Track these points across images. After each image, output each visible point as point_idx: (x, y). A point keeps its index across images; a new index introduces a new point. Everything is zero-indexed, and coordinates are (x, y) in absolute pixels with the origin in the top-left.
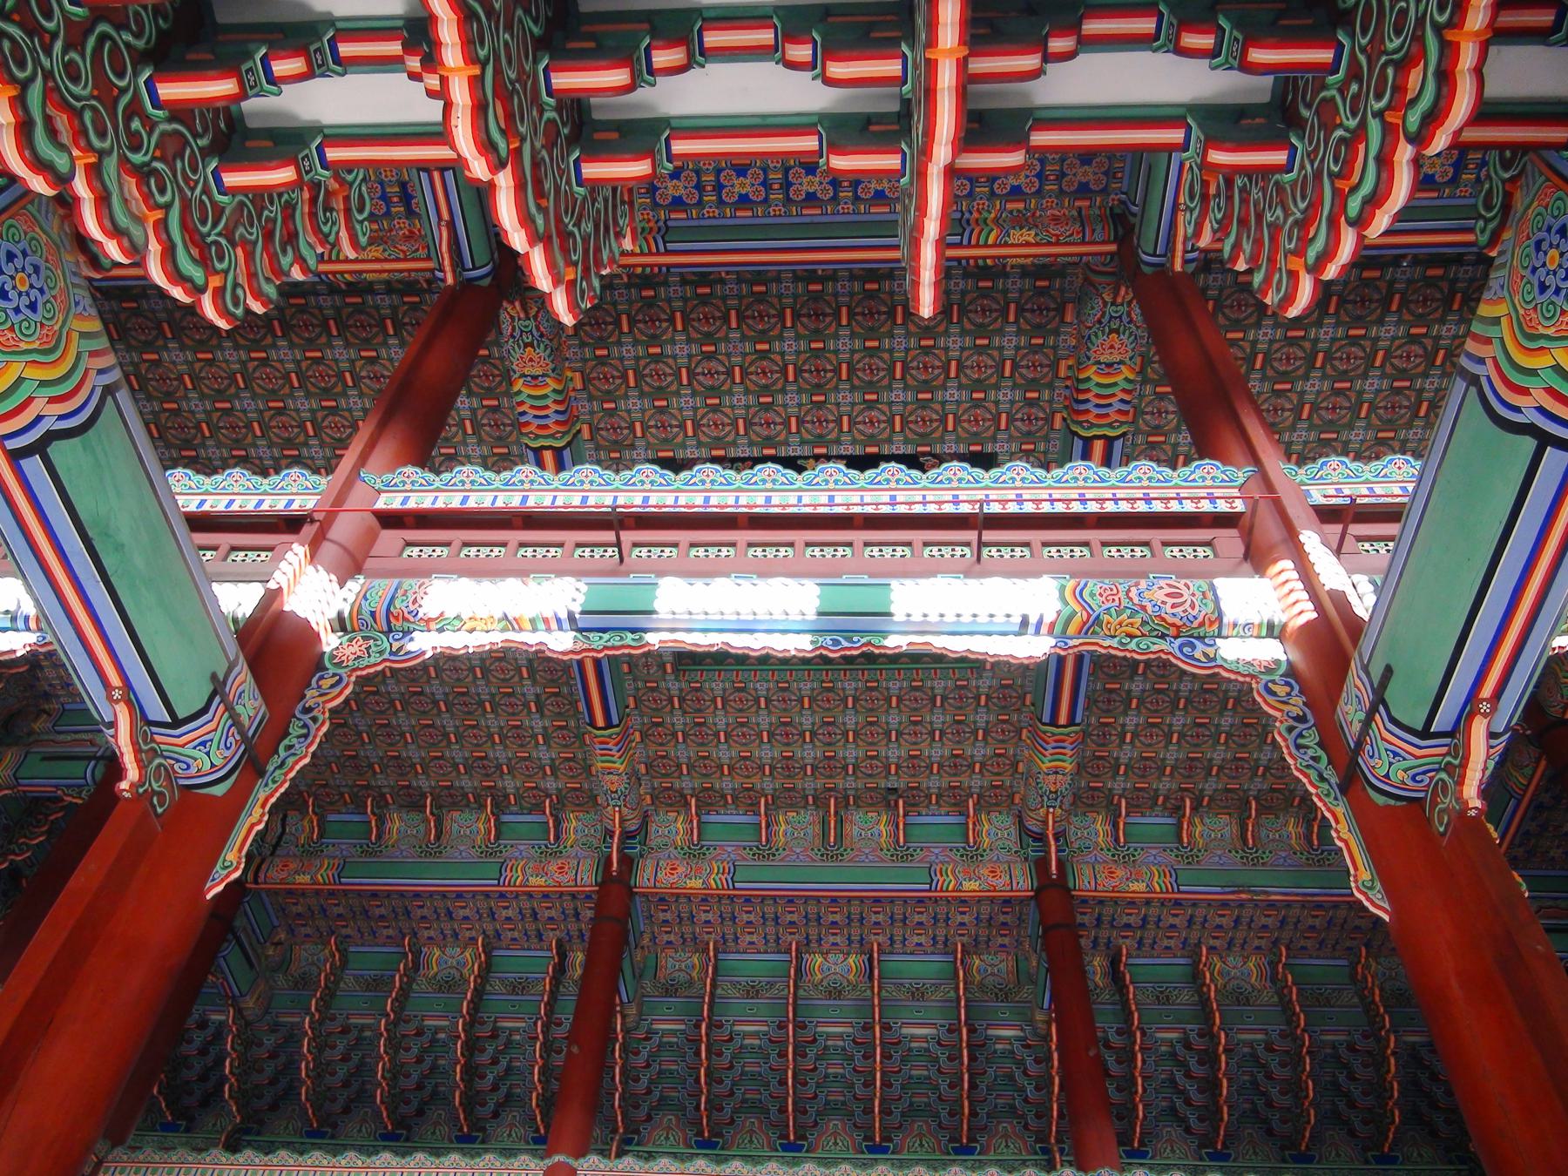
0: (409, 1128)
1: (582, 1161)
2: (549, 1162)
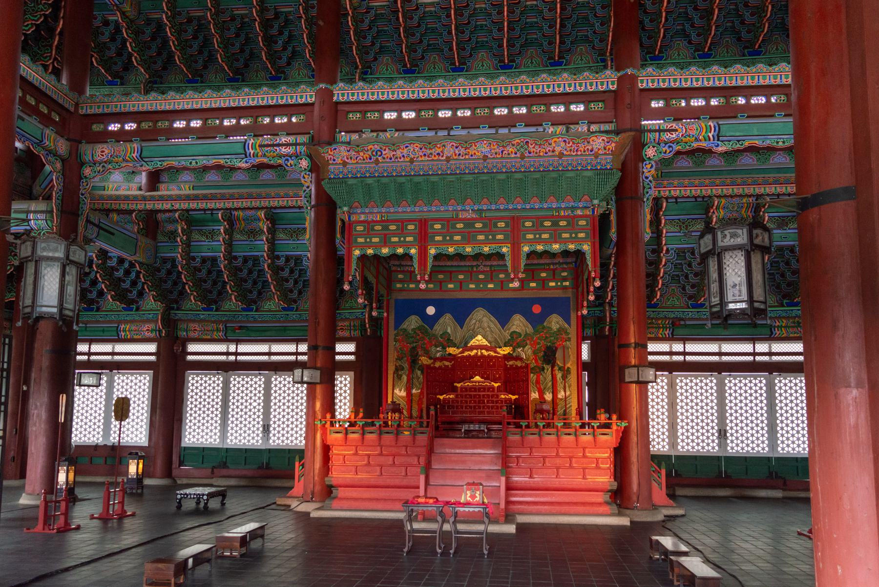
0: (242, 75)
1: (335, 86)
2: (317, 88)
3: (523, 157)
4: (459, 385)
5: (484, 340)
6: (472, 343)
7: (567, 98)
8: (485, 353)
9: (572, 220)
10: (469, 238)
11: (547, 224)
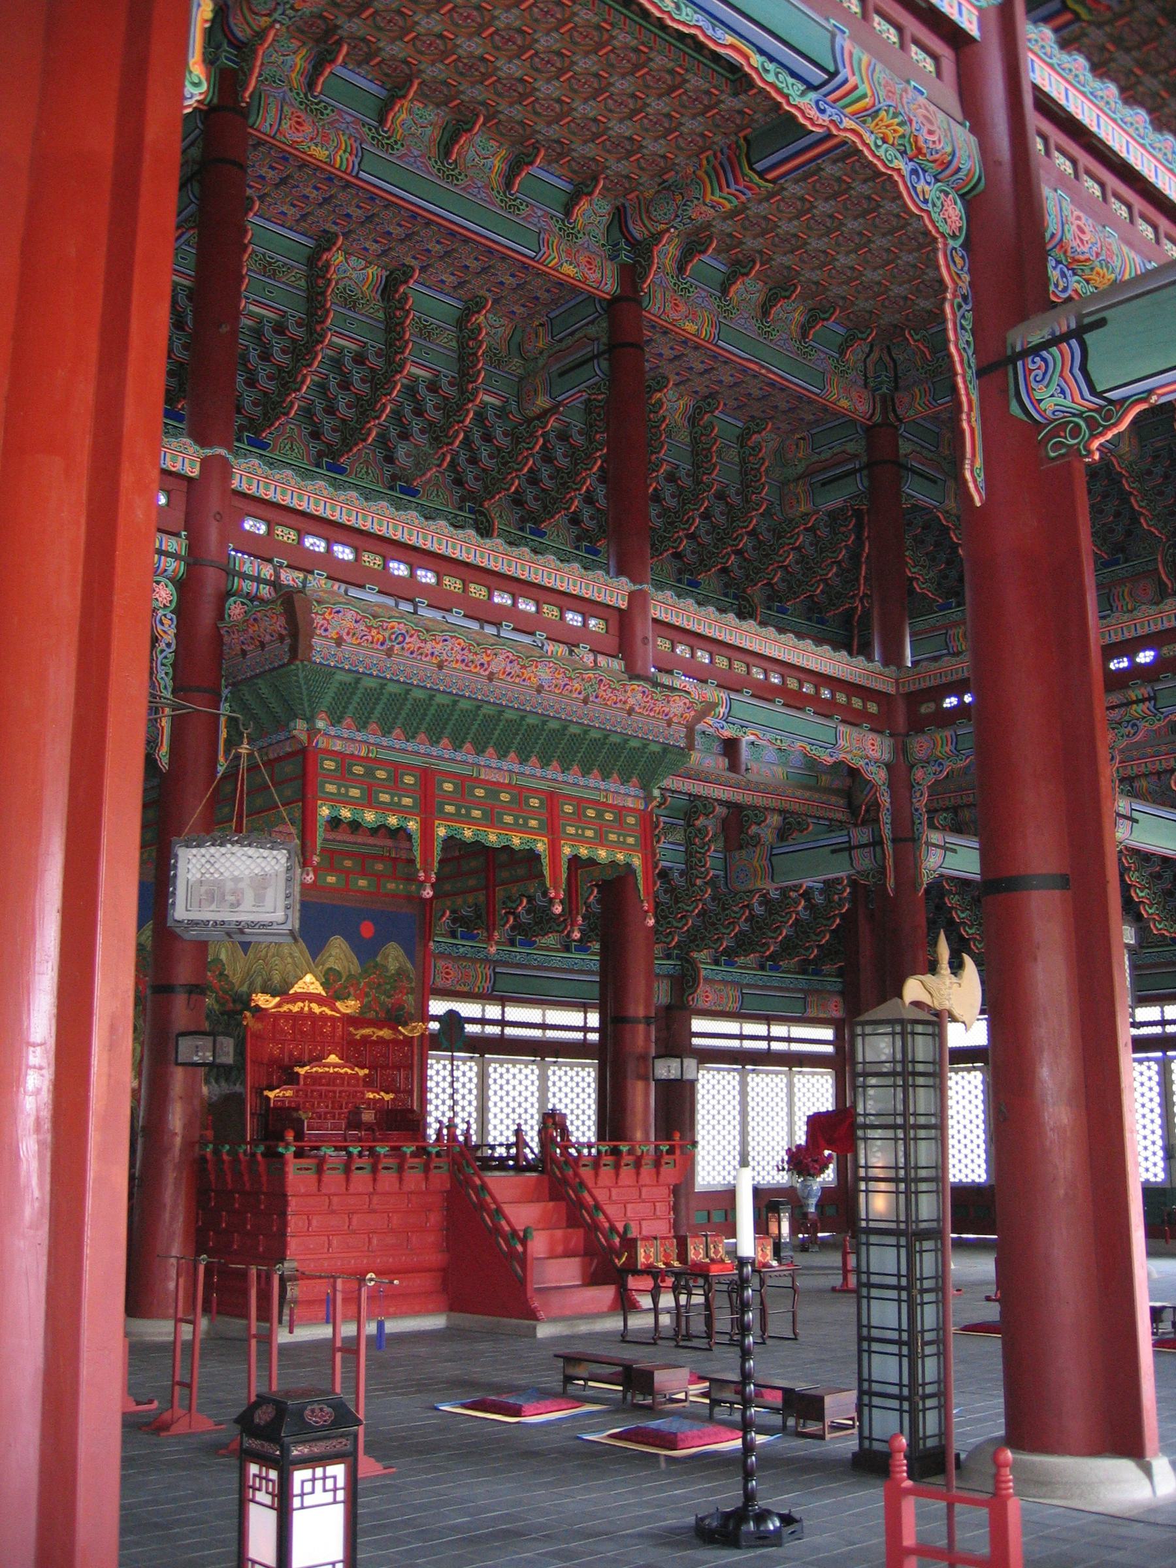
2: (209, 452)
3: (585, 701)
4: (302, 1071)
5: (317, 984)
6: (297, 988)
7: (333, 530)
8: (316, 1009)
9: (620, 811)
10: (492, 819)
11: (591, 813)
